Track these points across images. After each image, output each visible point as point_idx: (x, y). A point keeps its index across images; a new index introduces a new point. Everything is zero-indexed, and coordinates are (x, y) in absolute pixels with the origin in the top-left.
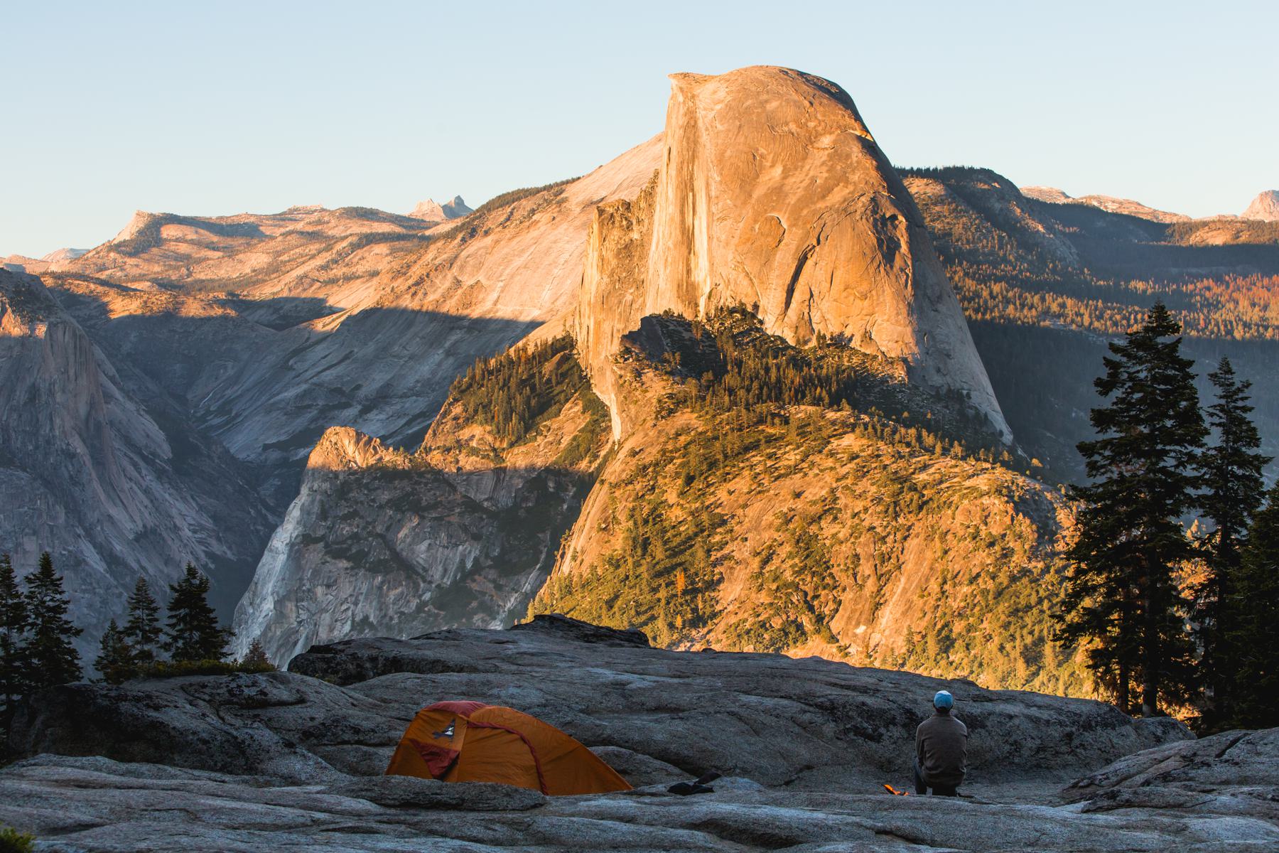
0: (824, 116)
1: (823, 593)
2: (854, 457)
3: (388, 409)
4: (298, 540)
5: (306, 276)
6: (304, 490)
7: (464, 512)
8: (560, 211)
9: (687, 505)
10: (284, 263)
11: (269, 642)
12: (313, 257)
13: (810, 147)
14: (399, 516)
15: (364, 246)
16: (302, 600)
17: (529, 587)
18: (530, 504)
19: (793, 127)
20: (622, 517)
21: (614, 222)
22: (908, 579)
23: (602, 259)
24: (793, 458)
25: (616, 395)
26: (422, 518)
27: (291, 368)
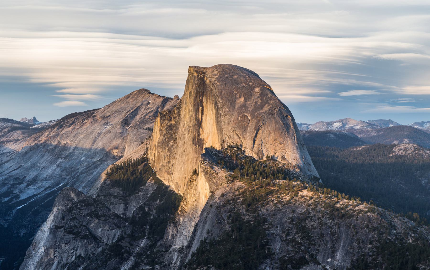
0: (254, 81)
1: (312, 246)
3: (36, 185)
4: (54, 227)
6: (55, 210)
7: (114, 218)
8: (93, 120)
9: (252, 215)
11: (42, 263)
13: (252, 91)
14: (91, 219)
17: (143, 245)
18: (140, 216)
19: (244, 84)
20: (225, 219)
21: (165, 118)
23: (161, 130)
24: (287, 198)
25: (204, 175)
26: (99, 220)
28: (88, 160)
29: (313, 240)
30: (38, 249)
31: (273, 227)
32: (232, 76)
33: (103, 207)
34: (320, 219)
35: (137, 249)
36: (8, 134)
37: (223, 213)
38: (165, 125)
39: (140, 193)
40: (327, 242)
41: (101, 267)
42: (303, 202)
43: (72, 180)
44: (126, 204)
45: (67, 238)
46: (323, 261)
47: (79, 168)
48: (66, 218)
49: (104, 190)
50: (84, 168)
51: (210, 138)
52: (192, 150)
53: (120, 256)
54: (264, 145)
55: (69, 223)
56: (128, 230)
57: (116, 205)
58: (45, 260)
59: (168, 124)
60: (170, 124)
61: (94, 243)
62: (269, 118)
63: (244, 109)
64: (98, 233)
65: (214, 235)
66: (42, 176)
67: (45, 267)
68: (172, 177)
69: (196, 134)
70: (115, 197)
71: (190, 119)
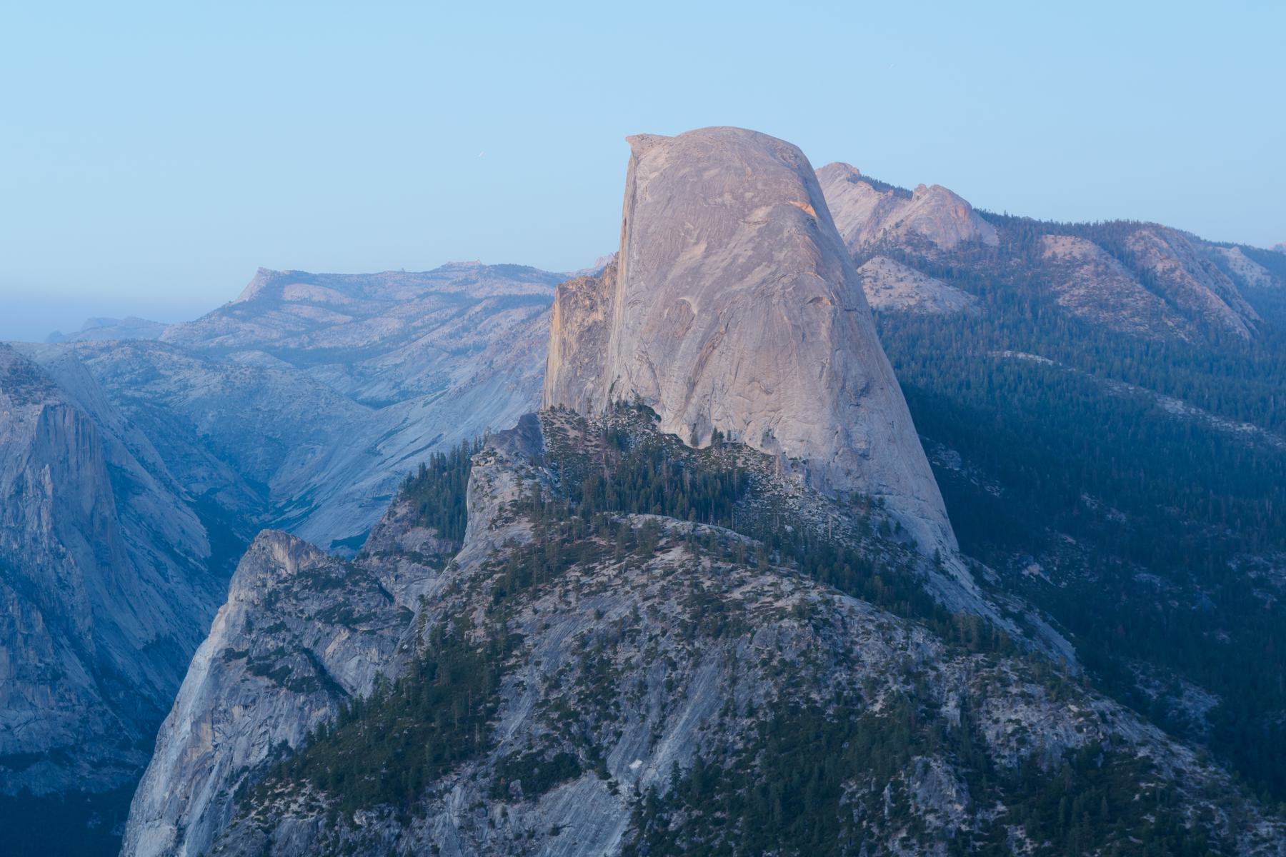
1: (605, 723)
4: (221, 655)
5: (430, 345)
7: (398, 625)
10: (416, 329)
11: (185, 768)
12: (443, 323)
14: (328, 629)
15: (499, 312)
16: (219, 722)
19: (728, 198)
21: (576, 302)
22: (693, 710)
23: (564, 343)
27: (379, 454)
30: (181, 724)
31: (526, 664)
36: (482, 320)
45: (249, 690)
46: (620, 769)
48: (257, 625)
49: (384, 535)
54: (717, 399)
57: (412, 582)
58: (192, 756)
59: (586, 324)
60: (590, 322)
61: (328, 704)
62: (752, 309)
63: (690, 280)
64: (347, 673)
67: (192, 779)
70: (416, 557)
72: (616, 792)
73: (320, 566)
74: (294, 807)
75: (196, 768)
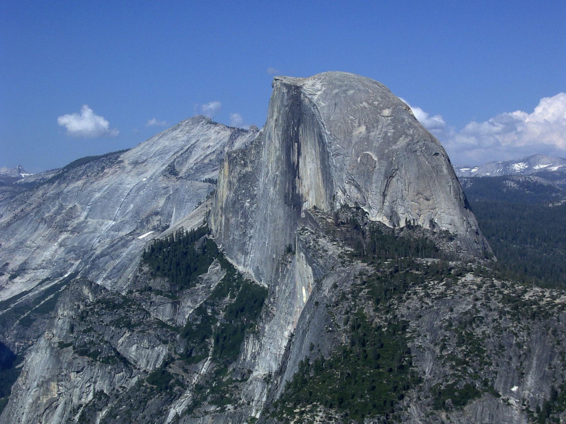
2: (480, 287)
7: (156, 328)
8: (120, 168)
11: (38, 407)
13: (378, 115)
14: (119, 330)
16: (62, 381)
17: (205, 371)
18: (199, 323)
19: (365, 104)
21: (236, 162)
23: (230, 182)
25: (304, 254)
28: (112, 233)
29: (487, 356)
32: (345, 91)
33: (138, 309)
34: (496, 321)
35: (196, 378)
37: (336, 315)
38: (236, 173)
39: (199, 286)
40: (510, 359)
41: (137, 409)
42: (467, 294)
43: (83, 267)
44: (176, 304)
45: (79, 364)
46: (505, 392)
47: (98, 246)
48: (76, 329)
49: (139, 281)
50: (105, 247)
51: (312, 193)
52: (284, 213)
53: (168, 391)
55: (81, 337)
56: (180, 346)
57: (160, 305)
58: (43, 400)
59: (242, 173)
60: (244, 172)
61: (124, 370)
63: (366, 143)
64: (131, 353)
65: (322, 351)
66: (35, 261)
68: (250, 259)
69: (289, 188)
70: (158, 293)
71: (278, 163)
72: (509, 404)
73: (108, 297)
74: (318, 418)
75: (46, 407)
